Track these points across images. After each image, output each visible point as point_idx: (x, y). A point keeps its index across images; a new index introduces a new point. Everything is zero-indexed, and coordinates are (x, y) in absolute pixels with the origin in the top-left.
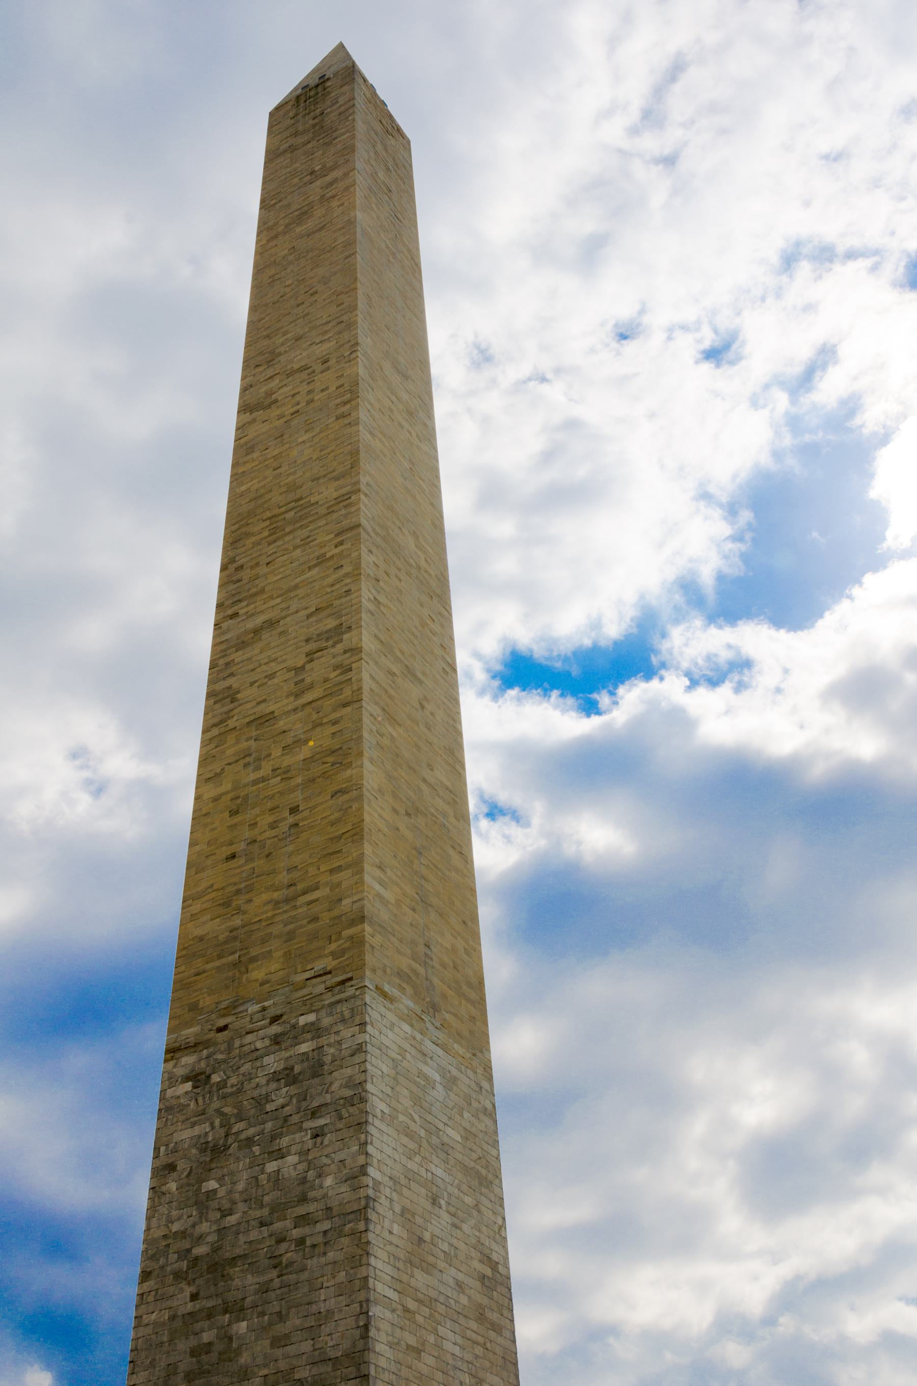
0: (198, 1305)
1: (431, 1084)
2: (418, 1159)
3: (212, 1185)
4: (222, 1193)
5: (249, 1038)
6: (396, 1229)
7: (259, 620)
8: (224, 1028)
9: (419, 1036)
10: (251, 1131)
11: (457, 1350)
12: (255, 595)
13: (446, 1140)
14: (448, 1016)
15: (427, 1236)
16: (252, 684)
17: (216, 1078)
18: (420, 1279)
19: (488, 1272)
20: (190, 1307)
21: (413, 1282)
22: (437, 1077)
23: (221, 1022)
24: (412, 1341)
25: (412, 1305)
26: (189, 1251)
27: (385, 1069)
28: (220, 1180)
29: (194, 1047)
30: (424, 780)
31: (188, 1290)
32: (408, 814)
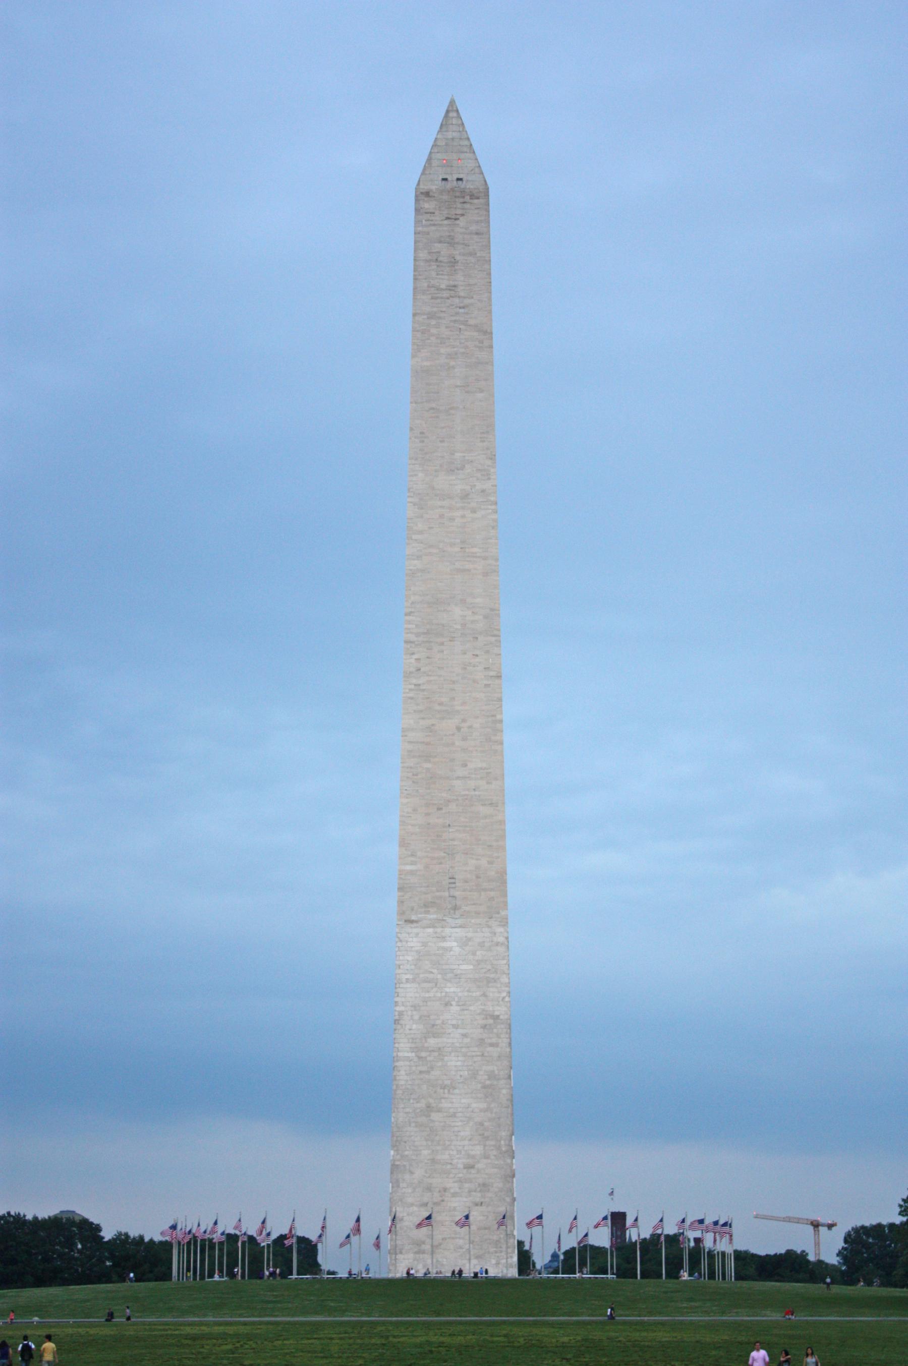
1: (450, 949)
2: (435, 990)
6: (414, 1026)
9: (439, 930)
11: (459, 1063)
13: (459, 972)
14: (467, 909)
15: (438, 1022)
18: (432, 1042)
19: (491, 1021)
21: (426, 1045)
22: (455, 944)
24: (424, 1068)
25: (423, 1054)
27: (410, 958)
30: (458, 778)
32: (439, 809)
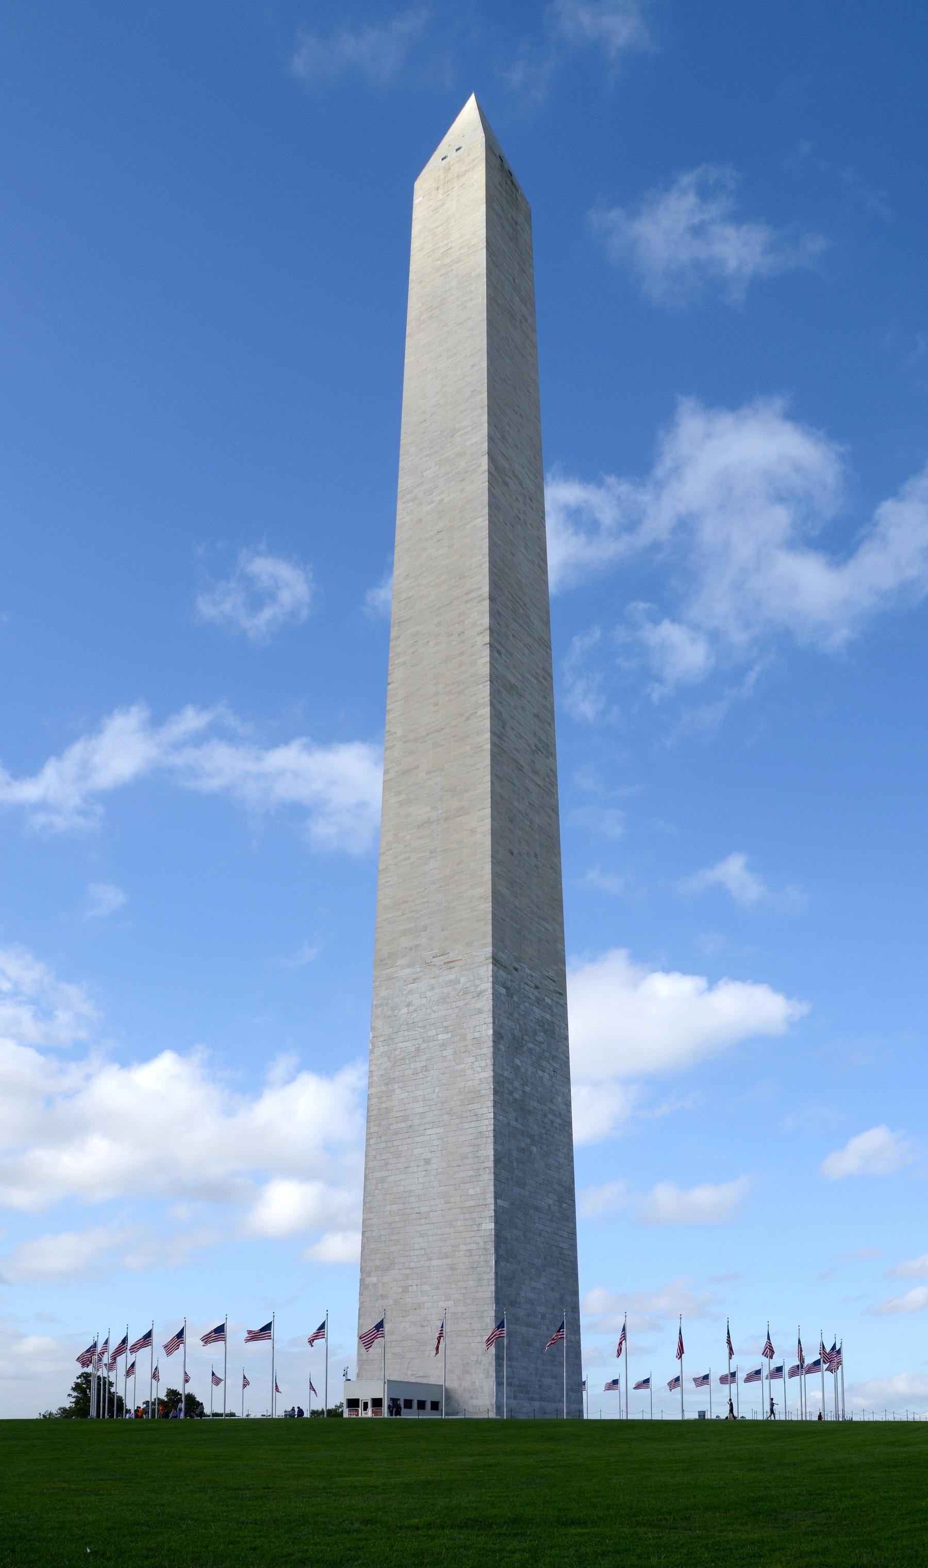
0: (518, 1126)
3: (518, 1062)
4: (523, 1070)
5: (527, 988)
7: (513, 680)
8: (516, 969)
10: (531, 1045)
12: (506, 649)
16: (513, 729)
17: (515, 998)
20: (513, 1123)
23: (517, 966)
26: (512, 1092)
28: (521, 1062)
29: (505, 968)
31: (514, 1114)
